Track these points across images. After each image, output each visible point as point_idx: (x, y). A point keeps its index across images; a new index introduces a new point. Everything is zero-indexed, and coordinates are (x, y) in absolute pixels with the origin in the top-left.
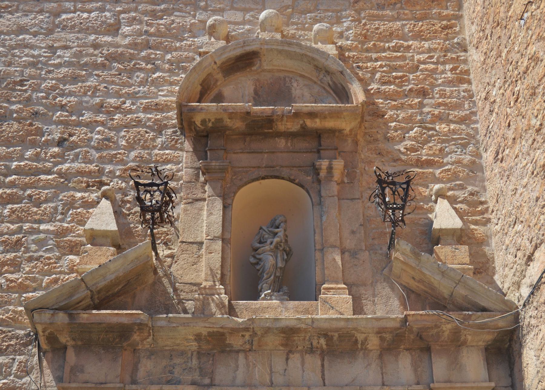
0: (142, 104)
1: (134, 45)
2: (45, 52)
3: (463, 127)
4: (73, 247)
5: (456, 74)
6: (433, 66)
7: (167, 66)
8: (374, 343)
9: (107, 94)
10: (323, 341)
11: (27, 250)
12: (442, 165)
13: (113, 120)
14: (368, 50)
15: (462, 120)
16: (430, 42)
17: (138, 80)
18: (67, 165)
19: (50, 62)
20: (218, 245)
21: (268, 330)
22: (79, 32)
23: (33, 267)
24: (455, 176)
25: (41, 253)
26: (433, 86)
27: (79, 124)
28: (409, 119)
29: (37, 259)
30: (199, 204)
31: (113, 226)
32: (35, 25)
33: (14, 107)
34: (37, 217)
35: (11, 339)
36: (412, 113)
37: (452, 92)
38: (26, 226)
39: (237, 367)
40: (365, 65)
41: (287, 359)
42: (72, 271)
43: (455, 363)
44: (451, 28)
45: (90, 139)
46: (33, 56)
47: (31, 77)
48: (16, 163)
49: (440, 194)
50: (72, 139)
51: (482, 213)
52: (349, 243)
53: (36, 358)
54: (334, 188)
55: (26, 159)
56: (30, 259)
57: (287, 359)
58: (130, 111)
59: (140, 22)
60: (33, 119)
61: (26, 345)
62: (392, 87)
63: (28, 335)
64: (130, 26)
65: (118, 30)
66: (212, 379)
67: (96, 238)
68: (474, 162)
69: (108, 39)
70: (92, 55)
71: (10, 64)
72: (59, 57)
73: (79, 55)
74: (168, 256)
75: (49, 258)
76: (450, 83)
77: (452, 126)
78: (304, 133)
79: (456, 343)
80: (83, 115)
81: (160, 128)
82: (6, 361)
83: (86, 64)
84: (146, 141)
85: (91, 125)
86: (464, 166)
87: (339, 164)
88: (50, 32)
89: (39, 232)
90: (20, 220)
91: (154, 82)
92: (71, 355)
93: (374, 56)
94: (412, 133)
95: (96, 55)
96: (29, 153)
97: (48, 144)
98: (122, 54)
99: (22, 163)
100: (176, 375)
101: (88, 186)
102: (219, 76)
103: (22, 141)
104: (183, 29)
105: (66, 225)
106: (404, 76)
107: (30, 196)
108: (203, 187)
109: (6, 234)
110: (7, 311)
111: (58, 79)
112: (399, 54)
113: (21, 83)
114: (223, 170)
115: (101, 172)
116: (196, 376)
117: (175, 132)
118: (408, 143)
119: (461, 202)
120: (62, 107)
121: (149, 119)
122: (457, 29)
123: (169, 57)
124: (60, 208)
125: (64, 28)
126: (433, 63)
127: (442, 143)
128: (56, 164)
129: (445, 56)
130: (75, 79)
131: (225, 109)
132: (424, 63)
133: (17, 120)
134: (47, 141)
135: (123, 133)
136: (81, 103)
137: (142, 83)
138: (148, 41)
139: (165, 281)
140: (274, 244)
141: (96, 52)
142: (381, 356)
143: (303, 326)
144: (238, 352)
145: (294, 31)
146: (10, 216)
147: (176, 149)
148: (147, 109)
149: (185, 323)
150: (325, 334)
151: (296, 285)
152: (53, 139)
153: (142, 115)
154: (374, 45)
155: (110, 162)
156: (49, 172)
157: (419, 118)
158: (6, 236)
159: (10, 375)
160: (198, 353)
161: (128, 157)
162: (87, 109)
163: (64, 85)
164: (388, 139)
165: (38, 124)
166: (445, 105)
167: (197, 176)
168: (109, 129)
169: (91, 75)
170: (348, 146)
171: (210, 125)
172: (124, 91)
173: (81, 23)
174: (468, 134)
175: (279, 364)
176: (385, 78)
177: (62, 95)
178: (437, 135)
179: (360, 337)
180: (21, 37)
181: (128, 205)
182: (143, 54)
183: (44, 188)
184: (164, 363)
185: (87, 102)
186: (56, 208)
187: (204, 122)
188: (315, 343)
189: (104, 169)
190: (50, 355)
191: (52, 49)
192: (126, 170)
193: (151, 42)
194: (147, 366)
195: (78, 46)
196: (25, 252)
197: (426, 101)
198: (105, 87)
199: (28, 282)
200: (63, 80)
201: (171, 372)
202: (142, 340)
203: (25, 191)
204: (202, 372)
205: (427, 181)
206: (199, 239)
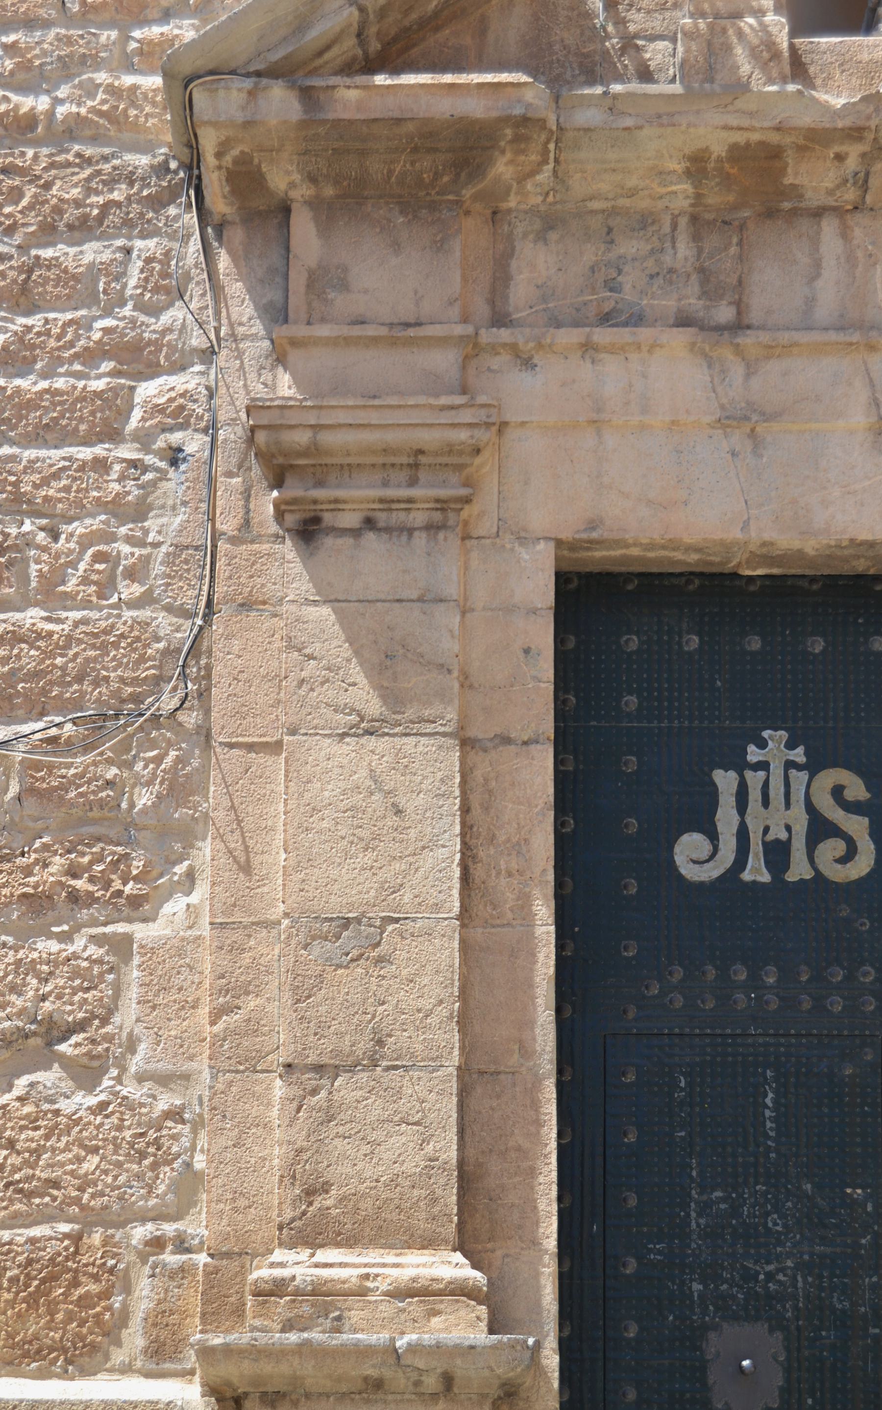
35: (111, 183)
39: (817, 265)
53: (195, 245)
61: (158, 202)
63: (162, 169)
66: (740, 306)
82: (106, 256)
100: (628, 294)
110: (91, 89)
144: (818, 213)
159: (122, 303)
160: (694, 219)
184: (590, 254)
190: (236, 234)
194: (536, 267)
201: (612, 286)
204: (711, 288)
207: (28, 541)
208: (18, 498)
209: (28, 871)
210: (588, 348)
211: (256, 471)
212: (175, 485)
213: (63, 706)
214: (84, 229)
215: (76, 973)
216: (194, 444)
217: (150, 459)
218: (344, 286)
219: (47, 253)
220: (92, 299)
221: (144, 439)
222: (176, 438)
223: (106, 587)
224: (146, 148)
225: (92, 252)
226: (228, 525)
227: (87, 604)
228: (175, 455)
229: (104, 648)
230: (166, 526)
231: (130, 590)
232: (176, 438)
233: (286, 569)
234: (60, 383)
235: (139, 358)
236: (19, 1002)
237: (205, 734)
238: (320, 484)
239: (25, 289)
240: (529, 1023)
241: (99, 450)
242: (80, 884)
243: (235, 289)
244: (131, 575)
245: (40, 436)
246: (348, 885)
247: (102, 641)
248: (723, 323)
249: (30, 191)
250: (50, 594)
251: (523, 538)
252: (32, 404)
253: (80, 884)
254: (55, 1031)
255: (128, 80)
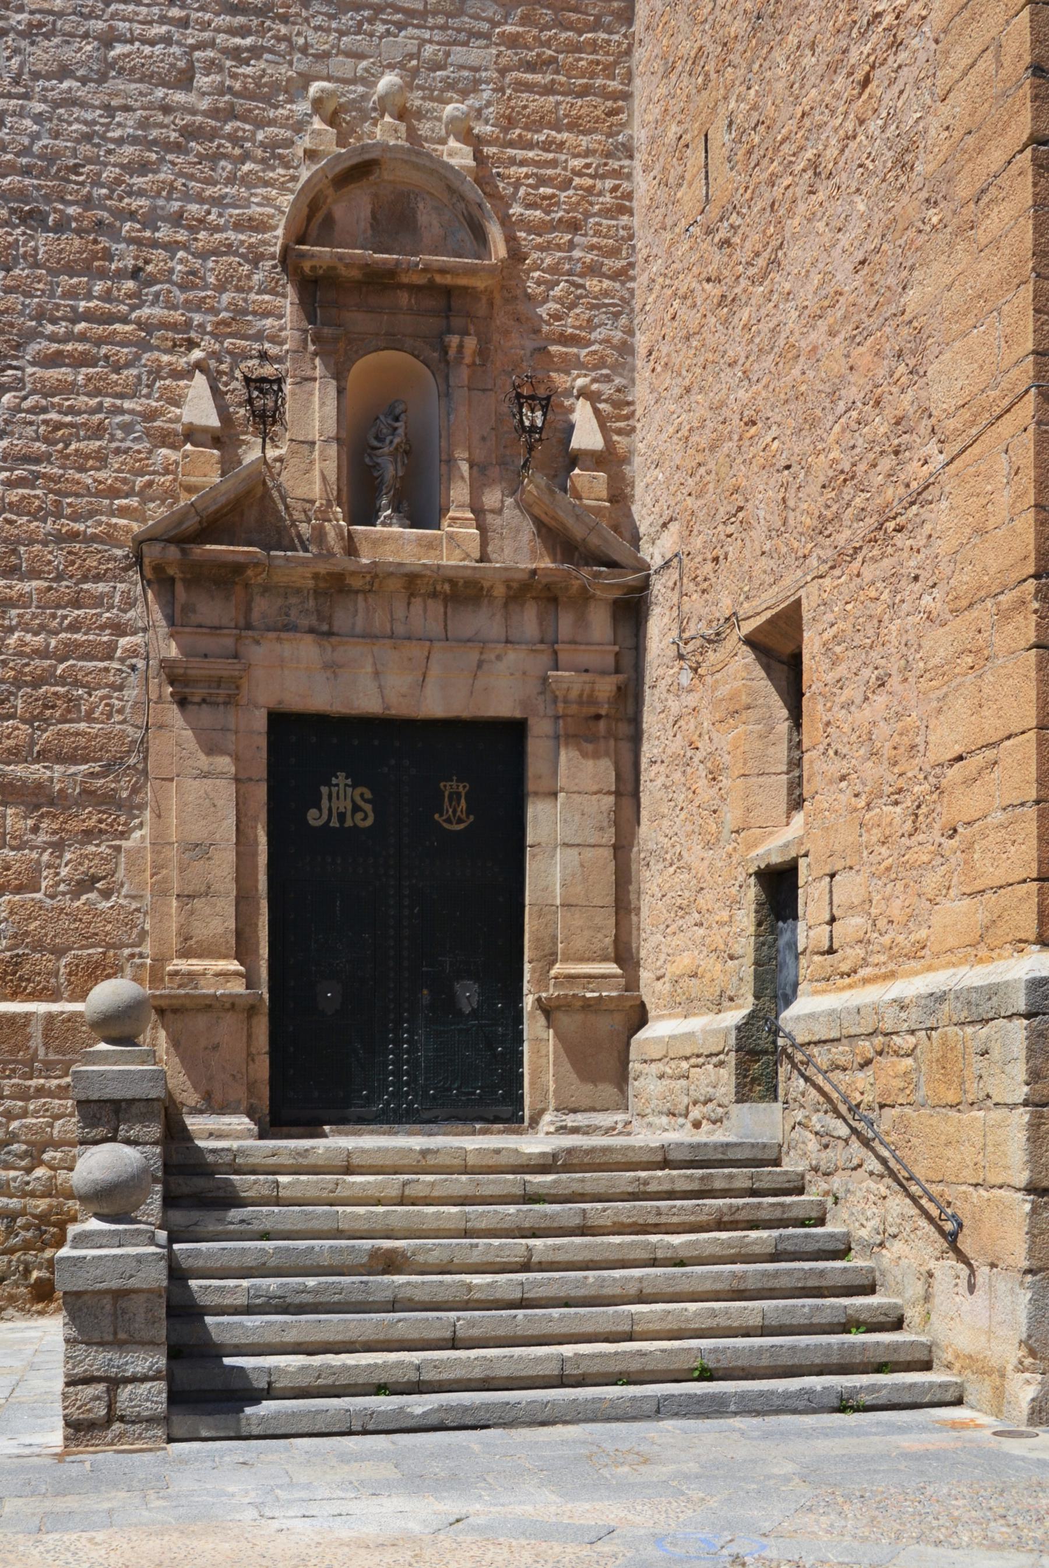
0: (231, 216)
1: (214, 113)
2: (100, 116)
3: (617, 285)
4: (164, 437)
5: (616, 198)
6: (590, 182)
7: (259, 152)
8: (500, 591)
9: (187, 197)
10: (447, 587)
11: (112, 439)
12: (589, 343)
13: (196, 239)
14: (511, 144)
15: (615, 276)
16: (589, 138)
17: (225, 175)
18: (146, 311)
19: (109, 135)
20: (333, 450)
21: (391, 574)
22: (141, 80)
23: (122, 464)
24: (602, 364)
25: (128, 444)
26: (587, 215)
27: (154, 244)
28: (554, 269)
29: (126, 452)
30: (309, 385)
31: (214, 422)
32: (81, 64)
33: (71, 210)
34: (118, 389)
35: (108, 560)
36: (560, 258)
37: (609, 227)
38: (108, 402)
40: (507, 172)
41: (409, 604)
42: (167, 472)
43: (582, 620)
44: (617, 114)
45: (171, 271)
46: (86, 123)
47: (89, 161)
48: (83, 304)
49: (583, 393)
50: (149, 268)
51: (628, 417)
52: (479, 455)
53: (139, 587)
54: (464, 373)
55: (95, 297)
56: (117, 451)
57: (409, 604)
58: (217, 229)
59: (221, 69)
60: (96, 232)
62: (538, 213)
63: (127, 557)
64: (207, 75)
65: (192, 78)
66: (330, 624)
67: (192, 434)
68: (624, 343)
69: (179, 97)
70: (162, 126)
71: (56, 135)
72: (119, 125)
73: (144, 124)
74: (276, 460)
75: (139, 452)
76: (607, 212)
77: (606, 283)
78: (431, 288)
79: (585, 597)
80: (158, 229)
81: (255, 259)
82: (107, 589)
83: (155, 142)
84: (239, 280)
85: (172, 247)
86: (613, 347)
87: (471, 343)
88: (103, 78)
89: (121, 411)
90: (97, 392)
91: (245, 181)
92: (179, 588)
93: (519, 154)
94: (557, 291)
95: (167, 126)
96: (98, 287)
97: (120, 275)
98: (200, 127)
99: (91, 304)
100: (293, 618)
101: (175, 345)
102: (330, 191)
103: (87, 270)
104: (276, 87)
105: (154, 404)
106: (554, 196)
107: (106, 357)
108: (313, 360)
109: (85, 412)
110: (100, 523)
111: (122, 166)
112: (550, 156)
113: (75, 169)
114: (336, 340)
115: (188, 324)
116: (313, 621)
117: (274, 267)
118: (553, 306)
119: (606, 401)
120: (132, 215)
121: (242, 242)
122: (624, 117)
123: (260, 136)
124: (144, 377)
125: (121, 71)
126: (590, 176)
127: (590, 309)
128: (133, 308)
129: (606, 164)
130: (144, 168)
131: (341, 258)
132: (580, 174)
133: (78, 232)
134: (118, 270)
135: (211, 265)
136: (154, 208)
137: (230, 181)
138: (232, 105)
139: (275, 494)
140: (394, 445)
141: (167, 120)
142: (506, 605)
143: (428, 573)
144: (357, 592)
145: (418, 102)
146: (86, 385)
147: (276, 294)
148: (238, 227)
149: (304, 562)
150: (452, 582)
151: (422, 512)
152: (126, 266)
153: (231, 235)
154: (520, 135)
155: (198, 309)
156: (125, 320)
157: (567, 267)
158: (85, 416)
160: (315, 591)
161: (219, 302)
162: (164, 219)
163: (131, 177)
164: (529, 297)
165: (104, 242)
166: (600, 248)
167: (305, 341)
168: (193, 254)
169: (162, 160)
170: (482, 309)
171: (321, 272)
172: (207, 193)
173: (143, 65)
174: (622, 299)
175: (400, 612)
176: (531, 197)
177: (130, 194)
178: (586, 296)
179: (486, 585)
180: (65, 85)
181: (225, 379)
182: (228, 128)
183: (122, 344)
184: (280, 602)
185: (163, 208)
186: (139, 377)
187: (313, 268)
188: (439, 588)
189: (191, 319)
190: (156, 586)
191: (109, 110)
192: (218, 324)
193: (237, 107)
194: (262, 606)
195: (143, 108)
196: (110, 441)
197: (577, 239)
198: (184, 185)
199: (118, 485)
200: (129, 168)
201: (287, 615)
202: (256, 576)
203: (99, 347)
204: (321, 618)
205: (568, 365)
206: (310, 438)
207: (80, 697)
208: (76, 680)
209: (84, 821)
210: (279, 639)
211: (164, 677)
212: (133, 679)
213: (95, 760)
214: (98, 578)
215: (102, 859)
216: (141, 664)
217: (124, 668)
218: (194, 611)
219: (85, 586)
220: (101, 605)
221: (122, 660)
222: (134, 661)
223: (110, 716)
224: (120, 547)
225: (102, 587)
226: (154, 697)
227: (103, 722)
228: (133, 668)
229: (109, 739)
230: (131, 694)
231: (118, 718)
232: (134, 661)
233: (174, 714)
234: (91, 637)
235: (119, 629)
236: (82, 869)
237: (145, 772)
238: (186, 686)
239: (77, 601)
240: (257, 881)
241: (106, 664)
242: (103, 826)
243: (155, 608)
244: (120, 711)
245: (83, 657)
246: (197, 831)
247: (109, 736)
248: (325, 634)
249: (79, 561)
250: (89, 718)
251: (257, 706)
252: (81, 645)
253: (103, 826)
254: (95, 879)
255: (114, 520)
